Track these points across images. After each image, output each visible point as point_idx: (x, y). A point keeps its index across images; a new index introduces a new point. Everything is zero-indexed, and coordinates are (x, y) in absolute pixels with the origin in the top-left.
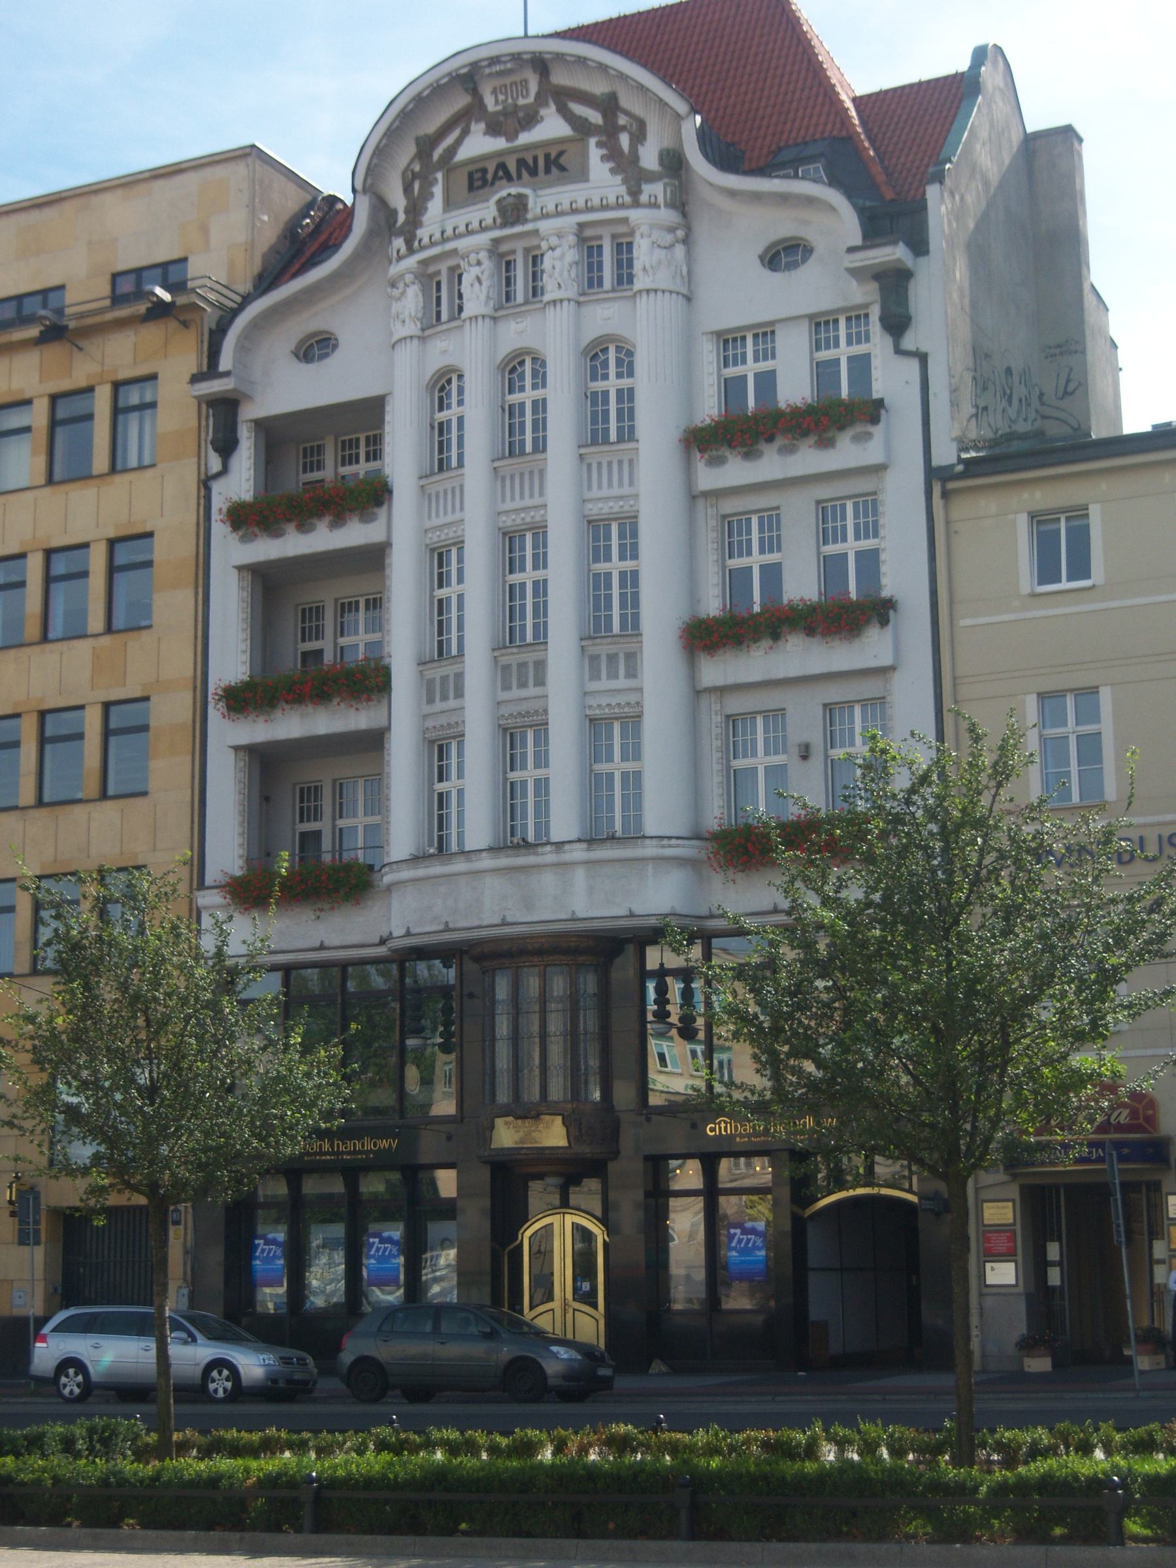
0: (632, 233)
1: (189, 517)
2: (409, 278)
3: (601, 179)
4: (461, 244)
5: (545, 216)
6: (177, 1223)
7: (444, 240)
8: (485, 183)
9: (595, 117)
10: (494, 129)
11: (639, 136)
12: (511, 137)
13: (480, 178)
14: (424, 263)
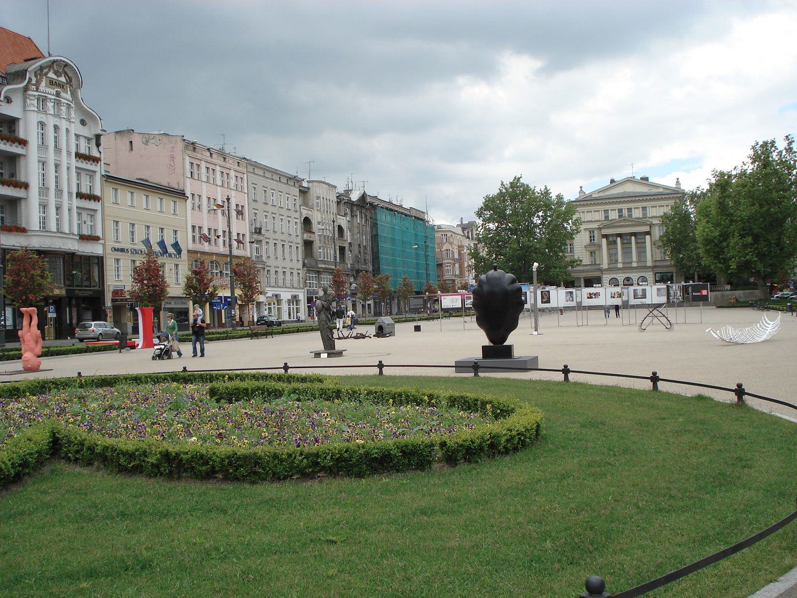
3: (68, 96)
10: (56, 73)
13: (52, 83)
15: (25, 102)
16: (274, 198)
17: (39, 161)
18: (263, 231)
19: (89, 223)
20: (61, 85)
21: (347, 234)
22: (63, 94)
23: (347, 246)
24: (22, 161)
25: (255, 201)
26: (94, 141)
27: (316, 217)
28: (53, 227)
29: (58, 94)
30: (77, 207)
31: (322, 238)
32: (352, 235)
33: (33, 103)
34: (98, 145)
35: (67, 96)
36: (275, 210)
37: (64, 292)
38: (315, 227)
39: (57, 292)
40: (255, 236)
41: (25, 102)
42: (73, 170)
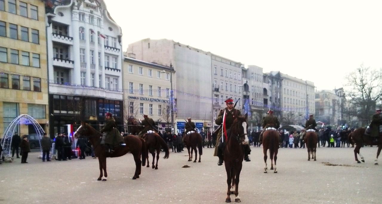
0: (101, 20)
1: (45, 30)
2: (78, 13)
4: (86, 13)
5: (95, 14)
6: (47, 126)
7: (83, 11)
8: (88, 6)
9: (99, 5)
11: (101, 9)
12: (91, 2)
13: (87, 6)
14: (80, 12)
15: (72, 16)
16: (231, 74)
17: (81, 49)
18: (220, 90)
19: (115, 83)
20: (94, 8)
21: (269, 93)
22: (95, 12)
23: (268, 98)
24: (71, 48)
25: (216, 74)
26: (117, 40)
27: (251, 83)
28: (97, 85)
29: (91, 12)
30: (106, 74)
31: (254, 94)
32: (272, 93)
33: (76, 17)
34: (120, 41)
35: (97, 14)
36: (227, 79)
37: (96, 119)
38: (250, 89)
39: (91, 118)
40: (215, 93)
41: (72, 16)
42: (103, 55)
